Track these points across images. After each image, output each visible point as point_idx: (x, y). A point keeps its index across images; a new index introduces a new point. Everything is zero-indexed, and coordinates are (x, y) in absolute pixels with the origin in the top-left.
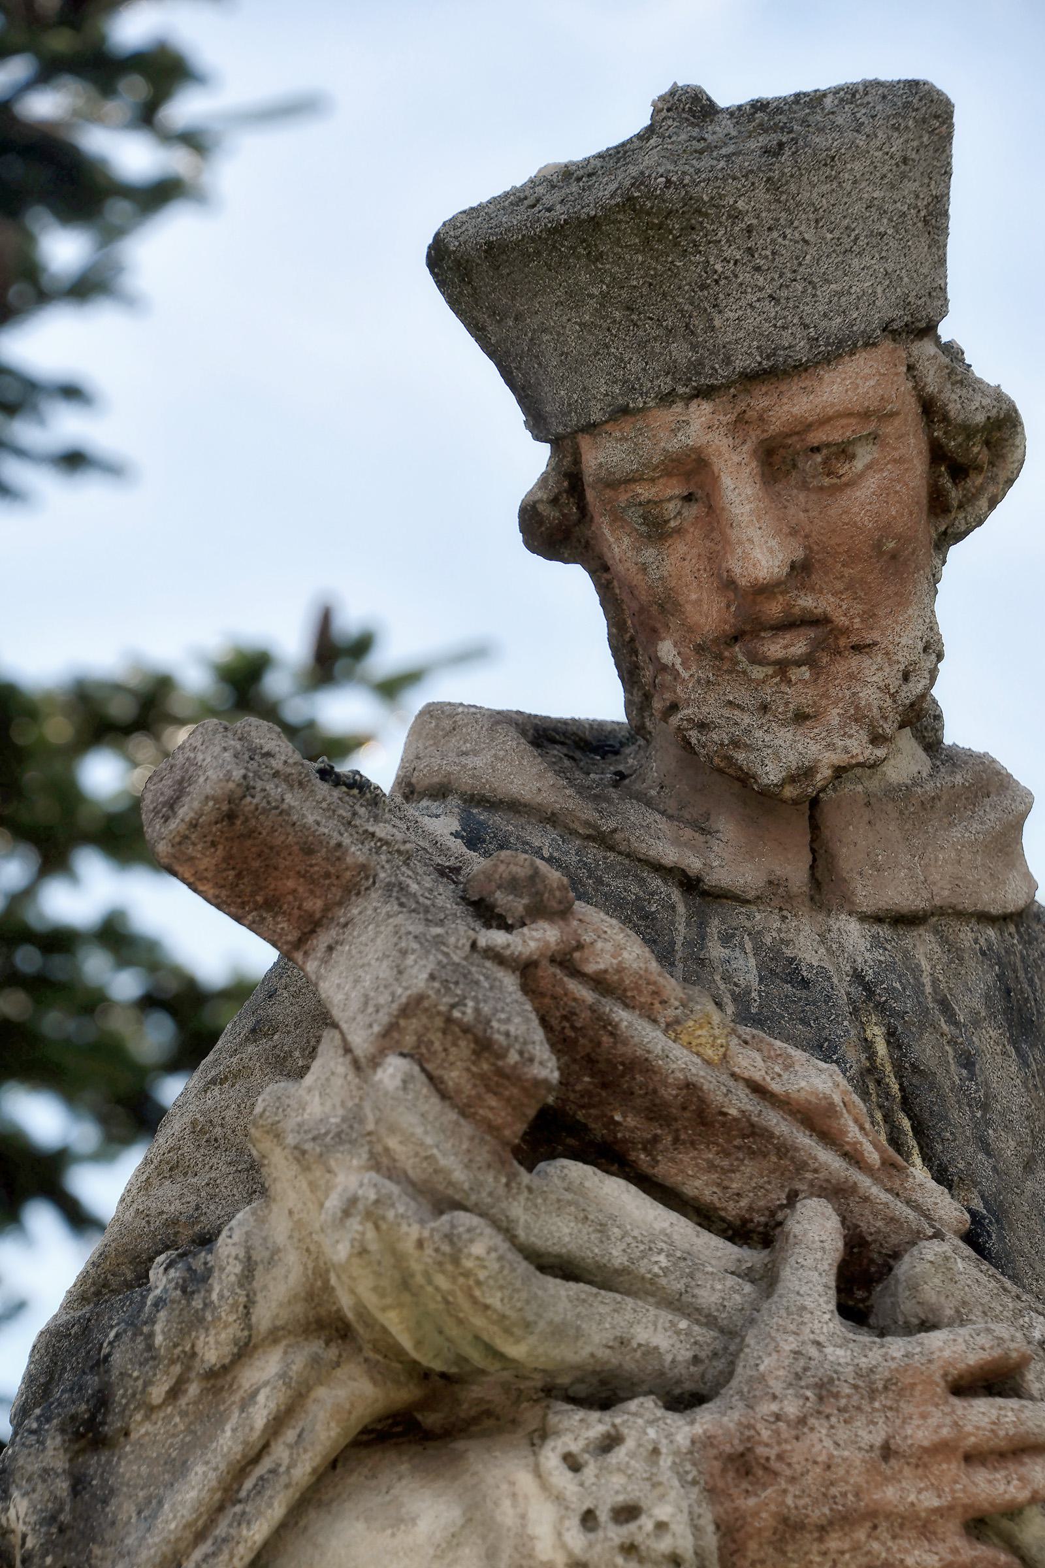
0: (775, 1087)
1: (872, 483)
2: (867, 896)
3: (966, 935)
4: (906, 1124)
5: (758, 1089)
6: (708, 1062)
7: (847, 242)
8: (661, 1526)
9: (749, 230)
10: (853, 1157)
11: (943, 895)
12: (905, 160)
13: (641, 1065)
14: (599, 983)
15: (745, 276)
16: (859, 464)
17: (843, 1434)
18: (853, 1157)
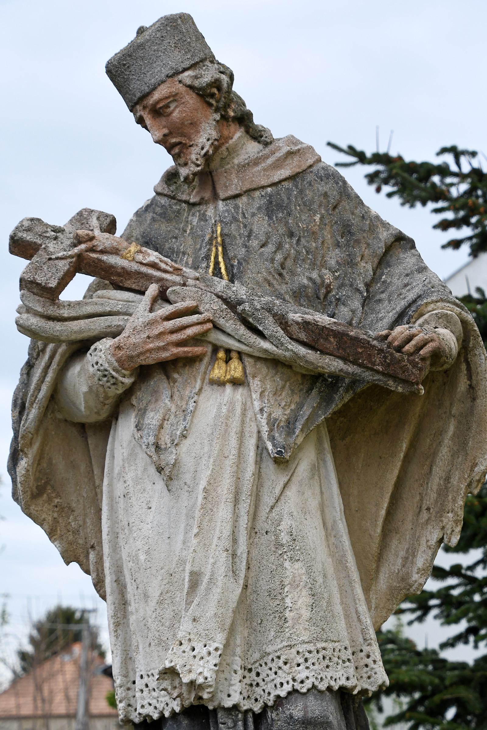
0: (144, 262)
1: (177, 111)
3: (257, 194)
4: (220, 249)
5: (141, 263)
6: (130, 261)
7: (151, 61)
8: (101, 365)
9: (128, 67)
10: (165, 271)
11: (247, 186)
12: (162, 37)
13: (111, 267)
14: (102, 252)
15: (131, 77)
16: (172, 108)
17: (137, 337)
18: (165, 271)
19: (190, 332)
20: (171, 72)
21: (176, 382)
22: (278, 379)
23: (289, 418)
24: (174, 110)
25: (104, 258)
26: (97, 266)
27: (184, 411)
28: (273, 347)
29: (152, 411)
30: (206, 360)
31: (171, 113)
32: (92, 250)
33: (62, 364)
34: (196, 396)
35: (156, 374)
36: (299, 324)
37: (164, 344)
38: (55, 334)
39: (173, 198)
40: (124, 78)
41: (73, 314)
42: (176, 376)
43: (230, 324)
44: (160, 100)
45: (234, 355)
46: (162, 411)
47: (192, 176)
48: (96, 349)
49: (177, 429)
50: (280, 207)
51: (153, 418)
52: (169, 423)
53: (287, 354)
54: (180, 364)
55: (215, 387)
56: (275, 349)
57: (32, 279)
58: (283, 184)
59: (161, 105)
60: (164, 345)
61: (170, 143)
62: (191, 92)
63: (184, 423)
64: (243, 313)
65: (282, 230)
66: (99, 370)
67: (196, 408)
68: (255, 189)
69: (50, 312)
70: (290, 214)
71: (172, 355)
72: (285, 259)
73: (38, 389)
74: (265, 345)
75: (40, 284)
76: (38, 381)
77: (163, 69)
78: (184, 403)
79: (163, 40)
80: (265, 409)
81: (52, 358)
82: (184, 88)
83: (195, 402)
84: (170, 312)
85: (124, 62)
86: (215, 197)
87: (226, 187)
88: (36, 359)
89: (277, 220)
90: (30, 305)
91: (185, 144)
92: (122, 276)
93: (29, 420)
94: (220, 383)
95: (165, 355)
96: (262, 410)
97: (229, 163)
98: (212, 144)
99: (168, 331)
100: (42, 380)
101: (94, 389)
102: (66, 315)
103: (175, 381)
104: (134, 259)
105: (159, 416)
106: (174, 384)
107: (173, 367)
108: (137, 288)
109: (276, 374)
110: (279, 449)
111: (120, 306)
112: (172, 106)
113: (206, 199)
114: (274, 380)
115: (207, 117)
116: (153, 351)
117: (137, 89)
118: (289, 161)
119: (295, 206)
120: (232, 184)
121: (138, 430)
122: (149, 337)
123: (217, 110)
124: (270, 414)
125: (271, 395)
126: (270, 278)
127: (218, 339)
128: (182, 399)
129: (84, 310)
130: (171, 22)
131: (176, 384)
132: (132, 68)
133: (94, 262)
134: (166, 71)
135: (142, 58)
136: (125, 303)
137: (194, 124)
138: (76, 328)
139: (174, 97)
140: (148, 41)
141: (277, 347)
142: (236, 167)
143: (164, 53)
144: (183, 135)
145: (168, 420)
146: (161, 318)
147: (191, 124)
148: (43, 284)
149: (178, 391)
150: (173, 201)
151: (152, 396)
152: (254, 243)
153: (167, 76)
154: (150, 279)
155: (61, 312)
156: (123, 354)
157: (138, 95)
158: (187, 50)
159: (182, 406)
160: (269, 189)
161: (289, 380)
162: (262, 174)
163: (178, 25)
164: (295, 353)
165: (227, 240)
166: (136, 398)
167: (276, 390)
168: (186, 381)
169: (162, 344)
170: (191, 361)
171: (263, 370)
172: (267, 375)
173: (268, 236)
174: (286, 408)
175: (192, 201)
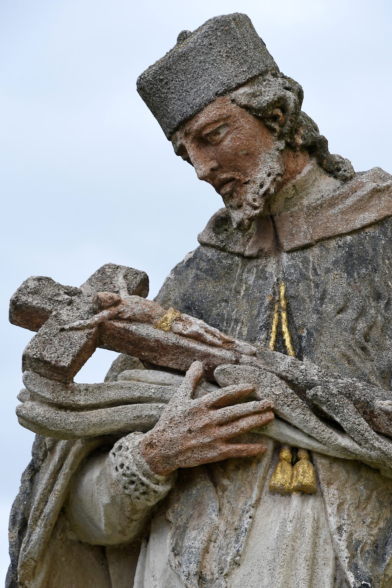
0: (185, 333)
1: (229, 138)
2: (287, 246)
3: (333, 244)
4: (284, 315)
5: (181, 334)
7: (195, 76)
8: (128, 468)
9: (166, 83)
10: (212, 345)
13: (142, 339)
14: (130, 320)
16: (222, 135)
17: (175, 430)
18: (212, 345)
19: (244, 424)
20: (221, 89)
21: (226, 490)
22: (362, 488)
23: (377, 540)
24: (224, 138)
25: (133, 327)
26: (123, 339)
27: (236, 529)
28: (355, 444)
29: (194, 529)
30: (265, 461)
31: (222, 141)
32: (117, 317)
33: (76, 467)
34: (252, 509)
35: (199, 480)
36: (389, 415)
37: (209, 440)
38: (67, 427)
39: (223, 249)
40: (160, 97)
41: (92, 401)
42: (226, 482)
43: (298, 414)
44: (207, 125)
45: (303, 455)
46: (207, 529)
47: (247, 221)
48: (120, 447)
49: (227, 554)
50: (363, 260)
51: (195, 539)
52: (216, 545)
53: (373, 454)
54: (231, 467)
55: (278, 497)
56: (357, 446)
57: (39, 355)
58: (367, 230)
59: (208, 131)
60: (210, 442)
61: (220, 180)
62: (247, 114)
63: (236, 546)
64: (315, 399)
65: (365, 290)
66: (124, 475)
67: (252, 525)
68: (330, 238)
69: (61, 399)
70: (376, 270)
71: (220, 454)
72: (370, 328)
73: (44, 500)
74: (344, 441)
75: (49, 363)
76: (44, 489)
77: (211, 85)
78: (236, 518)
79: (211, 49)
80: (345, 528)
81: (63, 459)
82: (239, 110)
83: (250, 517)
84: (218, 397)
85: (161, 77)
86: (278, 248)
87: (292, 235)
88: (43, 461)
89: (359, 277)
90: (36, 390)
91: (239, 181)
92: (156, 351)
93: (32, 543)
94: (284, 493)
95: (211, 454)
96: (340, 529)
97: (295, 205)
98: (274, 180)
99: (215, 422)
100: (49, 489)
101: (118, 500)
102: (82, 403)
103: (224, 489)
104: (171, 329)
105: (203, 536)
106: (223, 493)
107: (221, 470)
108: (175, 367)
109: (359, 480)
110: (363, 582)
111: (153, 391)
112: (223, 132)
113: (266, 250)
114: (356, 489)
115: (267, 146)
116: (196, 450)
117: (178, 111)
118: (375, 201)
119: (383, 259)
120: (300, 232)
121: (175, 555)
122: (190, 431)
123: (280, 137)
124: (351, 535)
125: (352, 509)
126: (350, 353)
127: (281, 434)
128: (233, 512)
129: (105, 395)
130: (222, 26)
131: (226, 493)
132: (171, 85)
133: (119, 333)
134: (214, 88)
135: (185, 72)
136: (159, 387)
137: (251, 156)
138: (94, 420)
139: (225, 121)
140: (192, 50)
141: (360, 445)
142: (305, 209)
143: (213, 64)
144: (236, 169)
145: (215, 542)
146: (206, 406)
147: (247, 154)
148: (53, 363)
149: (229, 502)
150: (222, 253)
151: (194, 509)
152: (329, 308)
153: (216, 94)
154: (192, 354)
155: (76, 398)
156: (156, 454)
157: (179, 118)
158: (242, 61)
159: (233, 523)
160: (349, 238)
161: (376, 489)
162: (339, 218)
163: (231, 28)
164: (383, 452)
165: (294, 304)
166: (173, 512)
167: (359, 501)
168: (239, 488)
169: (207, 440)
170: (245, 462)
171: (341, 475)
172: (347, 482)
173: (347, 298)
174: (373, 526)
175: (247, 253)
